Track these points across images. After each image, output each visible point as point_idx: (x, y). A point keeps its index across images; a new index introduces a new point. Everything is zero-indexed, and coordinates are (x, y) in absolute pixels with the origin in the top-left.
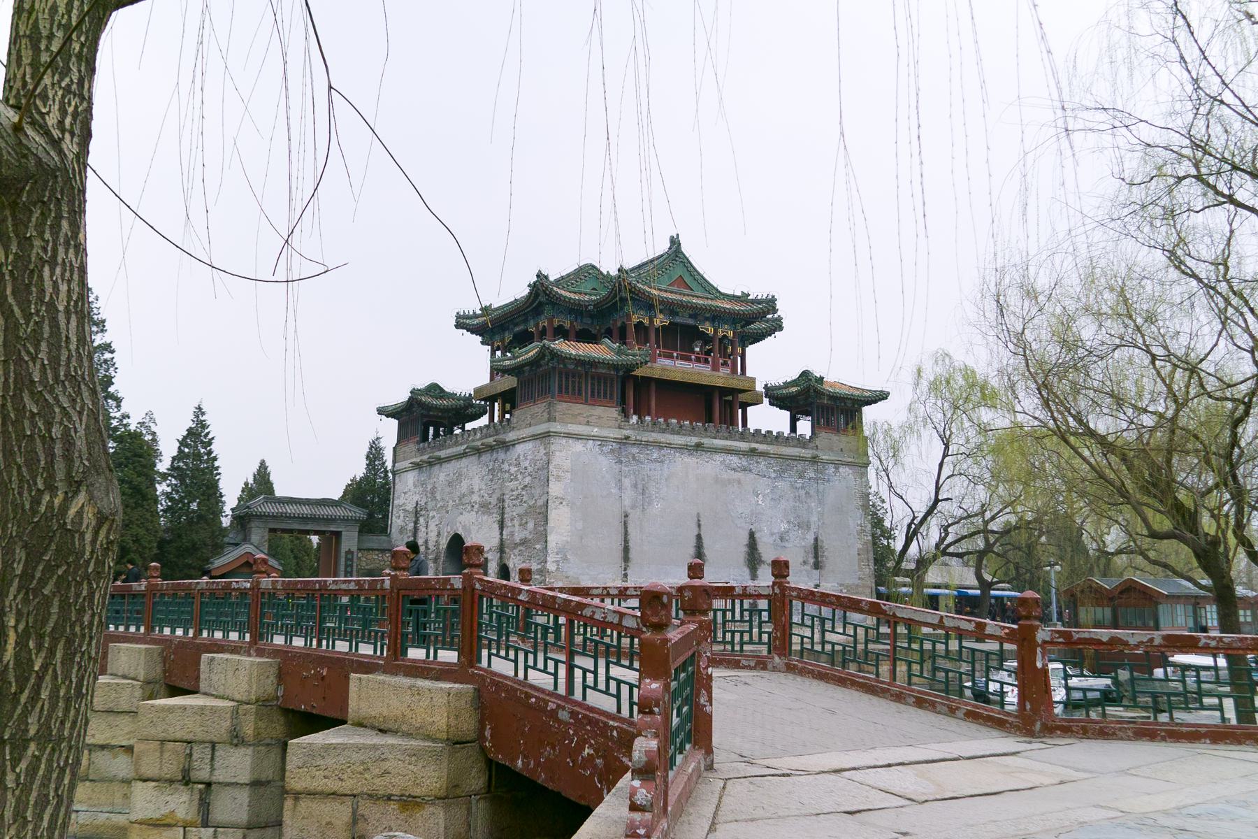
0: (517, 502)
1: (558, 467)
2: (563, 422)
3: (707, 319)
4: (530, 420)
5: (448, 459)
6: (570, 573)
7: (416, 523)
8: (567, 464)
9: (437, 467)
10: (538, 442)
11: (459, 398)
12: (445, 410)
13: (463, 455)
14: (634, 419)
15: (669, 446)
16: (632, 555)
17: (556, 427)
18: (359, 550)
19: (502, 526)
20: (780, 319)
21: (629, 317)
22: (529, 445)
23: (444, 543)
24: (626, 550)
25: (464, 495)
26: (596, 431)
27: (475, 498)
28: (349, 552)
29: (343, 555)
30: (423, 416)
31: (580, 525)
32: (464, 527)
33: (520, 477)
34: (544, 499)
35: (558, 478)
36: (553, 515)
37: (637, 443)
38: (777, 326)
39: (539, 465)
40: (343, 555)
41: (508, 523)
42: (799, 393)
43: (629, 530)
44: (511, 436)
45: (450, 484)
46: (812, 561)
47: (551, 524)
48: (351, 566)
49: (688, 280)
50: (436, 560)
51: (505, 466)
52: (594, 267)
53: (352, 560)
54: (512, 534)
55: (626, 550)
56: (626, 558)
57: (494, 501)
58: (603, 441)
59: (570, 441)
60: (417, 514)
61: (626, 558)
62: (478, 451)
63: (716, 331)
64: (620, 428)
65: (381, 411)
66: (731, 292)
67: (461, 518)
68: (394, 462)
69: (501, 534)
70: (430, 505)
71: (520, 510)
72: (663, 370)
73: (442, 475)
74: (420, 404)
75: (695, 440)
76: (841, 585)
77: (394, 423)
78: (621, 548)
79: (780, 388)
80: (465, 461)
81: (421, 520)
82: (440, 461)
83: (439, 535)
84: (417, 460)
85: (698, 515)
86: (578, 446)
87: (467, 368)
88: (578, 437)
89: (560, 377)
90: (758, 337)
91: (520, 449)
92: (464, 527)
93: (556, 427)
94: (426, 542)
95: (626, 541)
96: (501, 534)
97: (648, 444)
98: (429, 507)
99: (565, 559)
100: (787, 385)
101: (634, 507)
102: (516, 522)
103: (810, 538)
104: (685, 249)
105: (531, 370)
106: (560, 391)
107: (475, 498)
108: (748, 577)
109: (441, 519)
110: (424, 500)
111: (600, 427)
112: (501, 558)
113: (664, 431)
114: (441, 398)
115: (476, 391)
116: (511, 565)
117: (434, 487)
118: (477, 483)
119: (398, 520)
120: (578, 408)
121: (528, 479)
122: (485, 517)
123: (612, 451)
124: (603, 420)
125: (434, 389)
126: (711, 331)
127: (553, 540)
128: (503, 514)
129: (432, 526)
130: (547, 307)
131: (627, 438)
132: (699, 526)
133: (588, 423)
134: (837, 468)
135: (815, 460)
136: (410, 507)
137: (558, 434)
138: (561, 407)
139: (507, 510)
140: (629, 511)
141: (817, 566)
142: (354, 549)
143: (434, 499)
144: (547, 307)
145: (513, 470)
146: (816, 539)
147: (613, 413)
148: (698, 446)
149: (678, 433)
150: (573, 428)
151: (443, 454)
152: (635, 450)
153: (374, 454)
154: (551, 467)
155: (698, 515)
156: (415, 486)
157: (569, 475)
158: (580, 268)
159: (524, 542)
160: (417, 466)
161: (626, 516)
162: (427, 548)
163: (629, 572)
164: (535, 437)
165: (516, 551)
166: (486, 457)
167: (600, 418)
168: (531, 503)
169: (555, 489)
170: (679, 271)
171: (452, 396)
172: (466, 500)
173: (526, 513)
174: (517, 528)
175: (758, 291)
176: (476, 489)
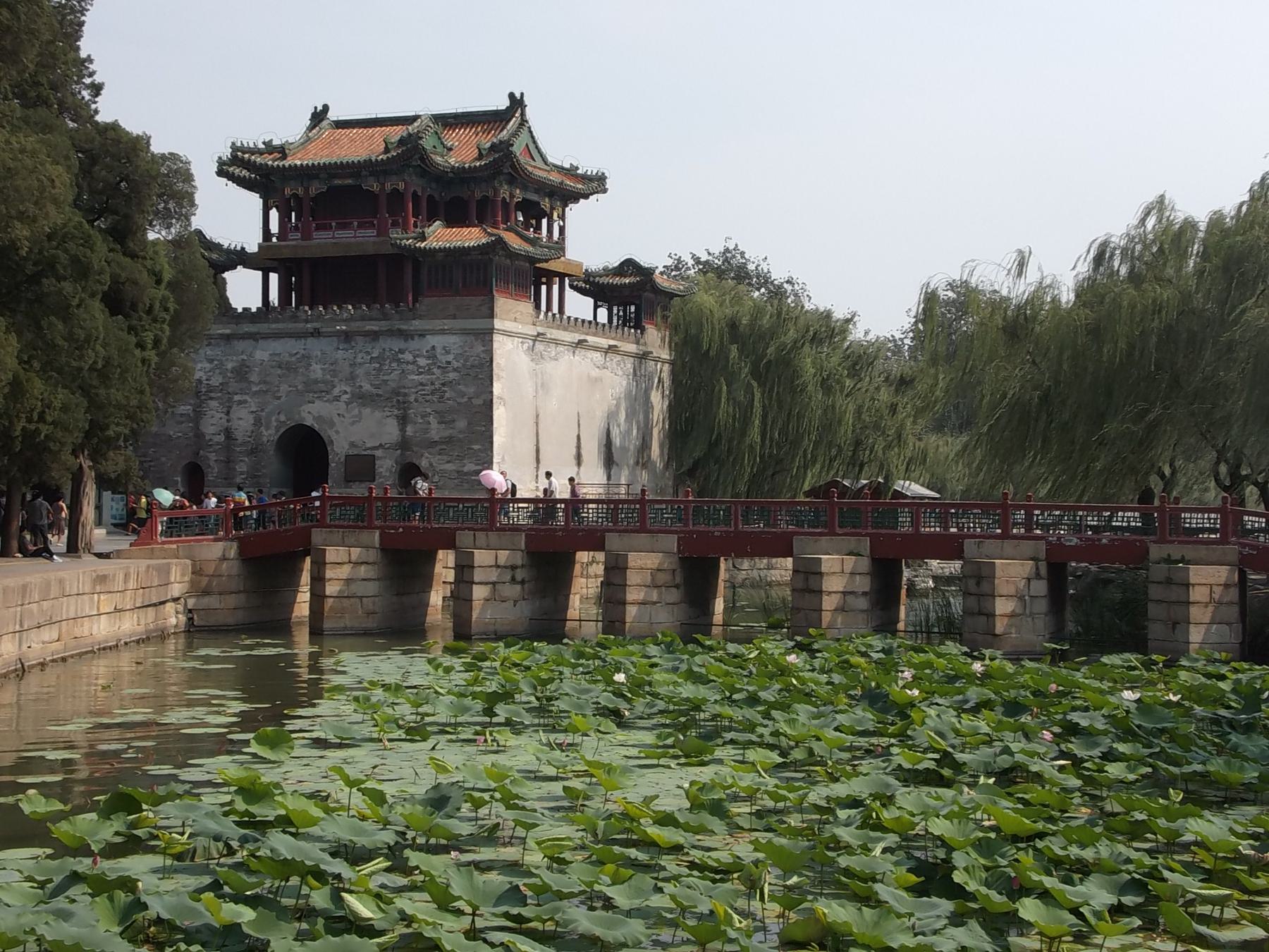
21: (496, 192)
66: (559, 163)
91: (433, 340)
169: (497, 388)
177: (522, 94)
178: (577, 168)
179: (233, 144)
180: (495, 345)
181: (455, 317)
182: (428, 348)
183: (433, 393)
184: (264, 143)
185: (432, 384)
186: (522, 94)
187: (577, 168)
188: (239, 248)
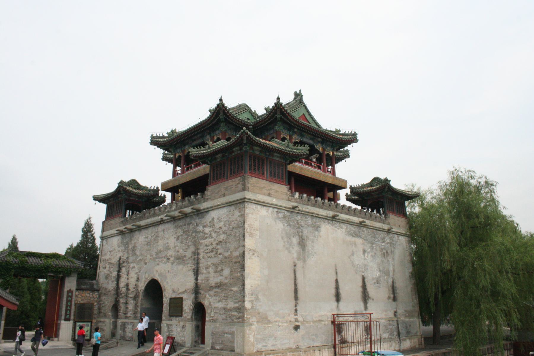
0: (212, 254)
1: (251, 226)
2: (253, 192)
3: (319, 142)
4: (216, 196)
5: (147, 227)
6: (261, 310)
7: (119, 271)
8: (256, 224)
9: (137, 233)
10: (233, 208)
11: (150, 190)
12: (139, 196)
13: (162, 222)
14: (297, 195)
15: (318, 217)
16: (300, 294)
17: (249, 195)
18: (77, 290)
19: (196, 273)
20: (347, 151)
22: (223, 212)
23: (142, 286)
24: (296, 291)
25: (160, 251)
26: (274, 201)
27: (171, 253)
28: (70, 291)
29: (65, 293)
30: (126, 199)
31: (266, 272)
32: (160, 275)
33: (214, 235)
34: (240, 250)
35: (251, 235)
36: (248, 263)
37: (300, 213)
38: (346, 155)
39: (233, 225)
40: (65, 293)
41: (203, 270)
42: (376, 190)
43: (297, 276)
44: (204, 205)
45: (148, 244)
46: (392, 296)
47: (247, 271)
48: (71, 301)
49: (308, 117)
50: (135, 298)
51: (200, 228)
52: (247, 106)
53: (71, 297)
54: (207, 279)
55: (296, 291)
56: (296, 298)
57: (189, 254)
58: (279, 208)
59: (259, 207)
60: (120, 266)
61: (296, 298)
62: (174, 219)
63: (324, 150)
64: (289, 200)
65: (95, 198)
67: (158, 268)
68: (103, 231)
69: (196, 279)
70: (131, 259)
71: (215, 260)
72: (301, 168)
73: (140, 238)
74: (125, 190)
75: (331, 213)
76: (406, 311)
77: (103, 207)
78: (293, 289)
79: (359, 188)
80: (161, 227)
81: (124, 270)
82: (140, 228)
83: (138, 279)
84: (122, 228)
85: (336, 265)
86: (263, 211)
87: (156, 172)
88: (263, 204)
89: (250, 159)
90: (339, 159)
91: (214, 214)
92: (160, 275)
93: (249, 195)
94: (127, 285)
95: (296, 285)
96: (196, 279)
97: (306, 214)
98: (130, 261)
99: (257, 299)
100: (364, 186)
101: (299, 259)
102: (211, 270)
103: (390, 281)
104: (305, 100)
105: (223, 156)
106: (250, 169)
107: (171, 253)
108: (363, 308)
109: (140, 269)
110: (126, 255)
111: (277, 198)
112: (196, 298)
113: (314, 205)
114: (138, 189)
115: (163, 185)
116: (206, 303)
117: (134, 247)
118: (172, 241)
119: (103, 270)
120: (263, 183)
121: (222, 237)
122: (181, 267)
123: (285, 217)
124: (279, 194)
125: (134, 183)
126: (321, 150)
127: (248, 283)
128: (198, 263)
129: (133, 275)
130: (223, 124)
131: (294, 208)
132: (336, 273)
133: (269, 195)
134: (398, 237)
135: (389, 231)
136: (115, 260)
137: (251, 201)
138: (253, 181)
139: (202, 261)
140: (297, 261)
141: (395, 299)
142: (74, 288)
143: (134, 254)
144: (223, 124)
145: (207, 230)
146: (393, 282)
147: (283, 189)
148: (334, 218)
149: (322, 208)
150: (261, 197)
151: (142, 223)
152: (299, 217)
153: (88, 229)
154: (246, 226)
155: (336, 265)
156: (119, 247)
157: (258, 233)
158: (240, 106)
159: (219, 286)
160: (121, 233)
161: (295, 266)
162: (128, 289)
163: (298, 308)
164: (230, 204)
165: (212, 293)
166: (180, 223)
167: (277, 191)
168: (227, 254)
169: (249, 243)
170: (302, 111)
171: (145, 188)
172: (160, 255)
173: (221, 262)
174: (212, 274)
175: (345, 128)
176: (172, 245)
177: (300, 91)
178: (340, 131)
179: (152, 135)
180: (247, 211)
181: (224, 195)
182: (210, 220)
183: (212, 251)
184: (168, 134)
185: (212, 244)
186: (300, 91)
187: (340, 131)
188: (155, 188)
